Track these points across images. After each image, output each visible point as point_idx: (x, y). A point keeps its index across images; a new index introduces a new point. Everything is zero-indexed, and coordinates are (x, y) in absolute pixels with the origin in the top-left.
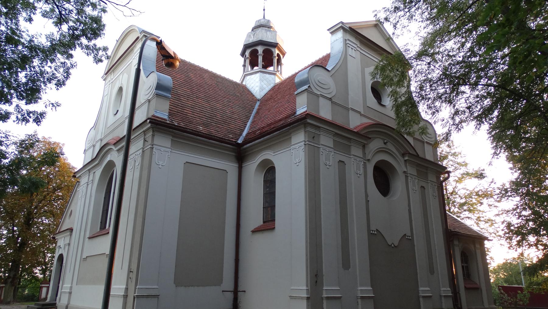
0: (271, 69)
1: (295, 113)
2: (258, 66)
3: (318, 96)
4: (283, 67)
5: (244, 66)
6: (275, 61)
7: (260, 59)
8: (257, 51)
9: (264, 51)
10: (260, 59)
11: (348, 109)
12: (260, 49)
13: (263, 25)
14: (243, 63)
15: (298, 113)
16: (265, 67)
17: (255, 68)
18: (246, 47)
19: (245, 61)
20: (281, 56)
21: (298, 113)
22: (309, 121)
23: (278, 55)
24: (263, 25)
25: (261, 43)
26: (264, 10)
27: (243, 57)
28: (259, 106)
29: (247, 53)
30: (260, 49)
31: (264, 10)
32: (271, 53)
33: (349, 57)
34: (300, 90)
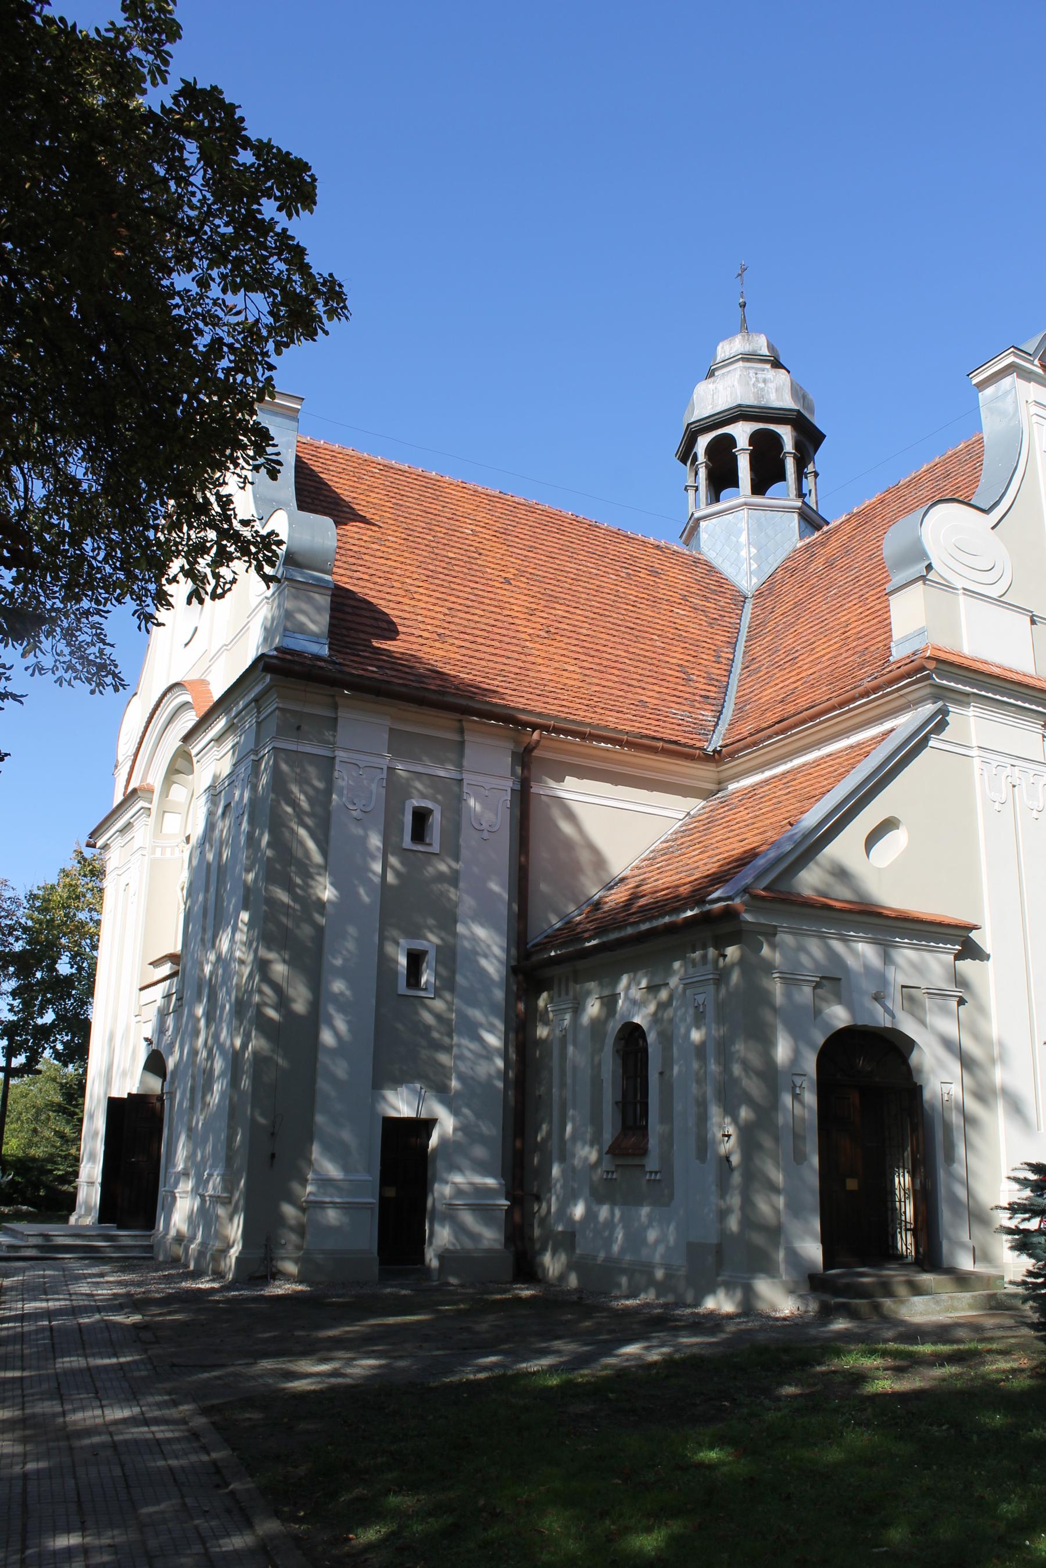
6: (790, 465)
8: (729, 441)
9: (755, 438)
12: (742, 432)
15: (898, 653)
21: (898, 653)
25: (741, 414)
27: (684, 460)
30: (742, 432)
32: (776, 440)
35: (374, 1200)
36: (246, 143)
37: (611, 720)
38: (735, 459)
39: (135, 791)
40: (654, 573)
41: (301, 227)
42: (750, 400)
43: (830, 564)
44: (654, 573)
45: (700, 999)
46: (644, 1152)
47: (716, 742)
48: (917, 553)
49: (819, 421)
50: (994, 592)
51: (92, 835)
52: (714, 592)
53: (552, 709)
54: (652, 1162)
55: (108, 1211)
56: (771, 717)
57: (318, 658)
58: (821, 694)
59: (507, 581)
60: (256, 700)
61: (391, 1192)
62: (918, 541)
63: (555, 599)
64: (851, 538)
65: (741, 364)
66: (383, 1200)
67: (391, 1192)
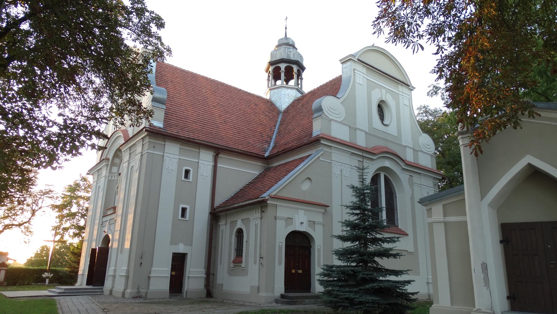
0: (292, 83)
1: (311, 134)
2: (280, 79)
3: (331, 120)
4: (303, 80)
5: (268, 80)
6: (295, 76)
7: (283, 75)
8: (279, 68)
9: (286, 68)
10: (283, 75)
11: (356, 129)
12: (283, 66)
13: (287, 43)
14: (267, 78)
16: (287, 81)
17: (279, 82)
18: (271, 63)
19: (269, 76)
20: (301, 71)
22: (322, 142)
23: (298, 71)
24: (287, 43)
25: (282, 61)
26: (286, 28)
27: (267, 71)
28: (282, 119)
29: (271, 69)
30: (283, 66)
31: (286, 28)
33: (357, 84)
34: (315, 115)
35: (169, 275)
36: (148, 11)
37: (240, 147)
38: (280, 73)
39: (103, 159)
40: (256, 105)
41: (161, 33)
42: (285, 57)
43: (303, 106)
44: (256, 105)
45: (257, 222)
46: (241, 262)
47: (266, 155)
48: (320, 109)
49: (305, 64)
50: (339, 120)
51: (89, 171)
52: (272, 111)
53: (224, 144)
54: (243, 265)
55: (90, 281)
56: (282, 148)
57: (160, 128)
58: (295, 144)
59: (214, 106)
60: (142, 138)
61: (174, 273)
62: (321, 106)
63: (227, 112)
64: (309, 99)
65: (284, 46)
66: (171, 276)
67: (174, 273)
